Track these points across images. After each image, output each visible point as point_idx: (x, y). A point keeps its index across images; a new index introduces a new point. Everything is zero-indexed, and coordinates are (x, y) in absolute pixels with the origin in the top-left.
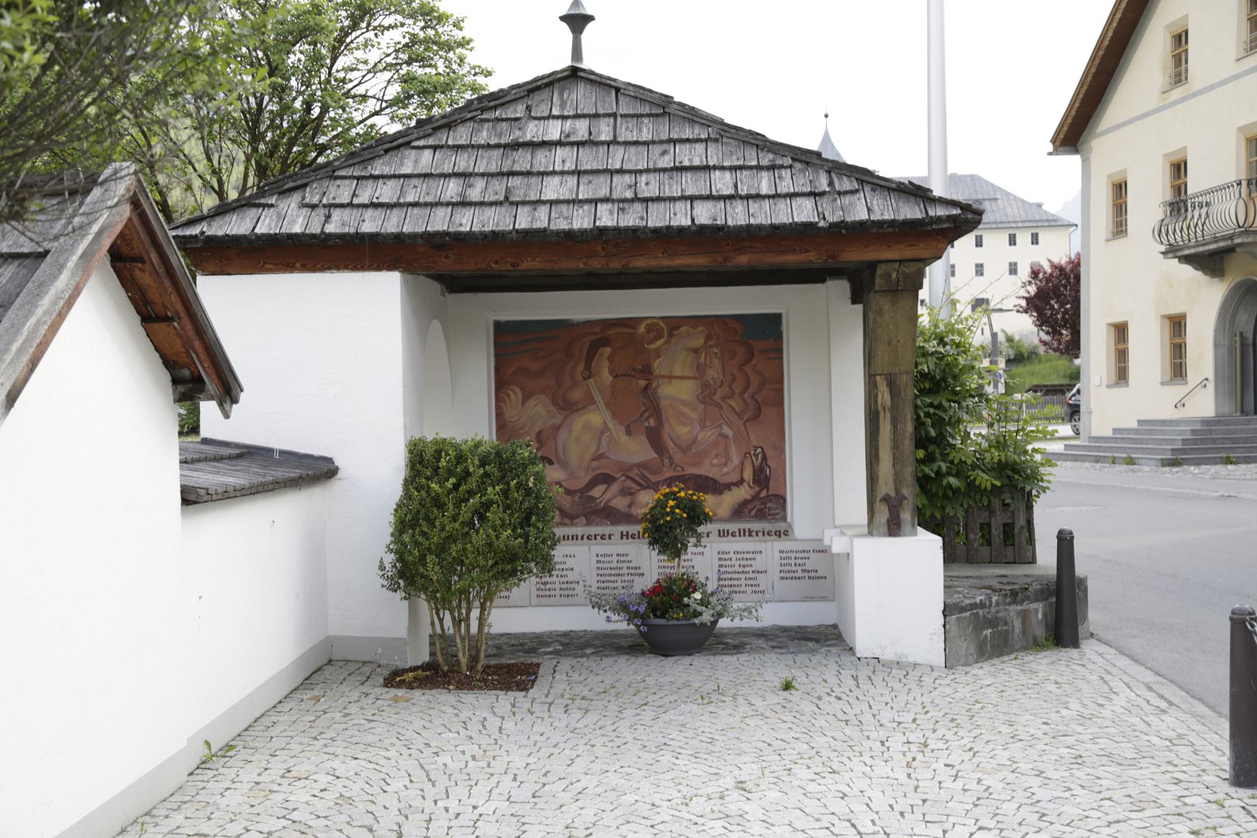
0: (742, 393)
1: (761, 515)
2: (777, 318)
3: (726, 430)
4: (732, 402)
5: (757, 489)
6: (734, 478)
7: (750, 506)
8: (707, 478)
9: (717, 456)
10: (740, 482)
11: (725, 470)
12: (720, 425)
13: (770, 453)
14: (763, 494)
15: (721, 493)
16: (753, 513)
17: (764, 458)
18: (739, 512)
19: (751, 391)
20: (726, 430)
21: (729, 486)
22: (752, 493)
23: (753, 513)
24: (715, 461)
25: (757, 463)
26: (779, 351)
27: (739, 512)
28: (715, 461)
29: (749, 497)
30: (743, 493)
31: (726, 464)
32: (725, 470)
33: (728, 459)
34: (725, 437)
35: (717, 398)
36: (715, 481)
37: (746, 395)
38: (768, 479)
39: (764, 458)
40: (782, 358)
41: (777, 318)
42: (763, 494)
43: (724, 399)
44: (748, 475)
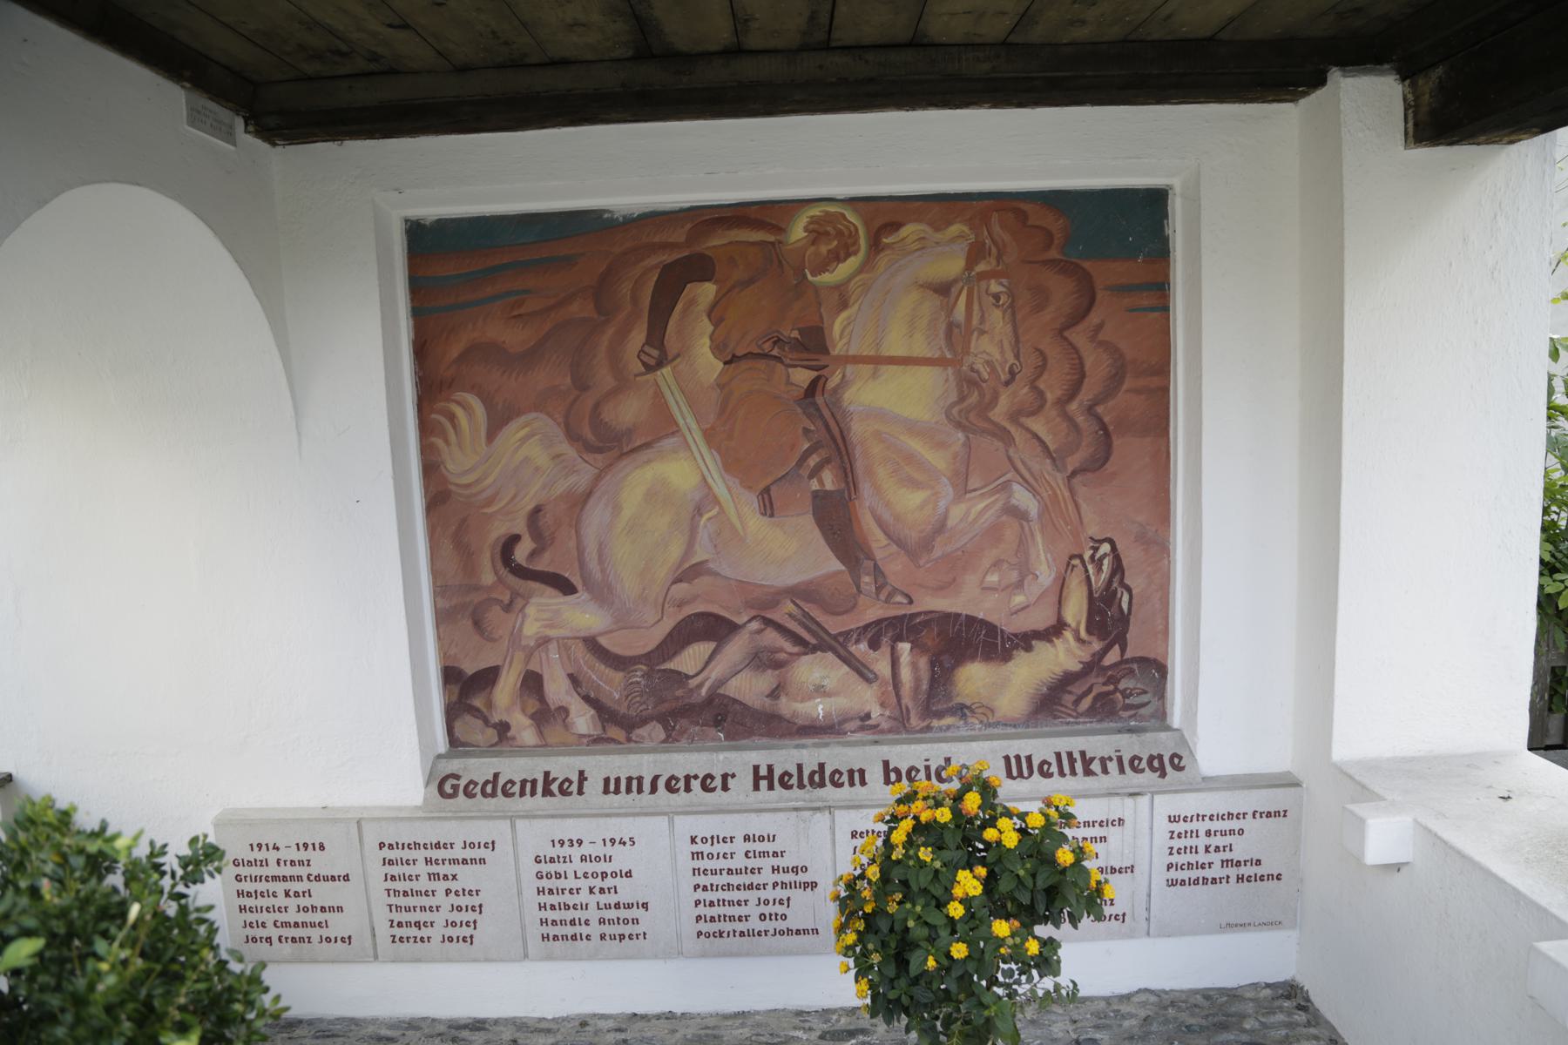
0: (1062, 403)
1: (1105, 709)
2: (1150, 205)
3: (1022, 497)
4: (1037, 425)
5: (1097, 646)
6: (1040, 619)
7: (1078, 689)
8: (971, 620)
9: (997, 564)
10: (1056, 630)
11: (1019, 599)
12: (1006, 487)
13: (1130, 556)
14: (1113, 657)
15: (1006, 657)
16: (1086, 703)
17: (1118, 568)
18: (1050, 703)
19: (1085, 395)
20: (1022, 497)
21: (1026, 641)
22: (1084, 654)
23: (1086, 703)
24: (993, 578)
25: (1099, 581)
26: (1160, 289)
27: (1050, 703)
28: (993, 578)
29: (1074, 666)
30: (1062, 656)
31: (1019, 585)
32: (1019, 599)
33: (1025, 571)
34: (1019, 514)
35: (999, 413)
36: (991, 629)
37: (1073, 406)
38: (1124, 620)
39: (1118, 568)
40: (1164, 308)
41: (1150, 205)
42: (1113, 657)
43: (1015, 417)
44: (1075, 610)
